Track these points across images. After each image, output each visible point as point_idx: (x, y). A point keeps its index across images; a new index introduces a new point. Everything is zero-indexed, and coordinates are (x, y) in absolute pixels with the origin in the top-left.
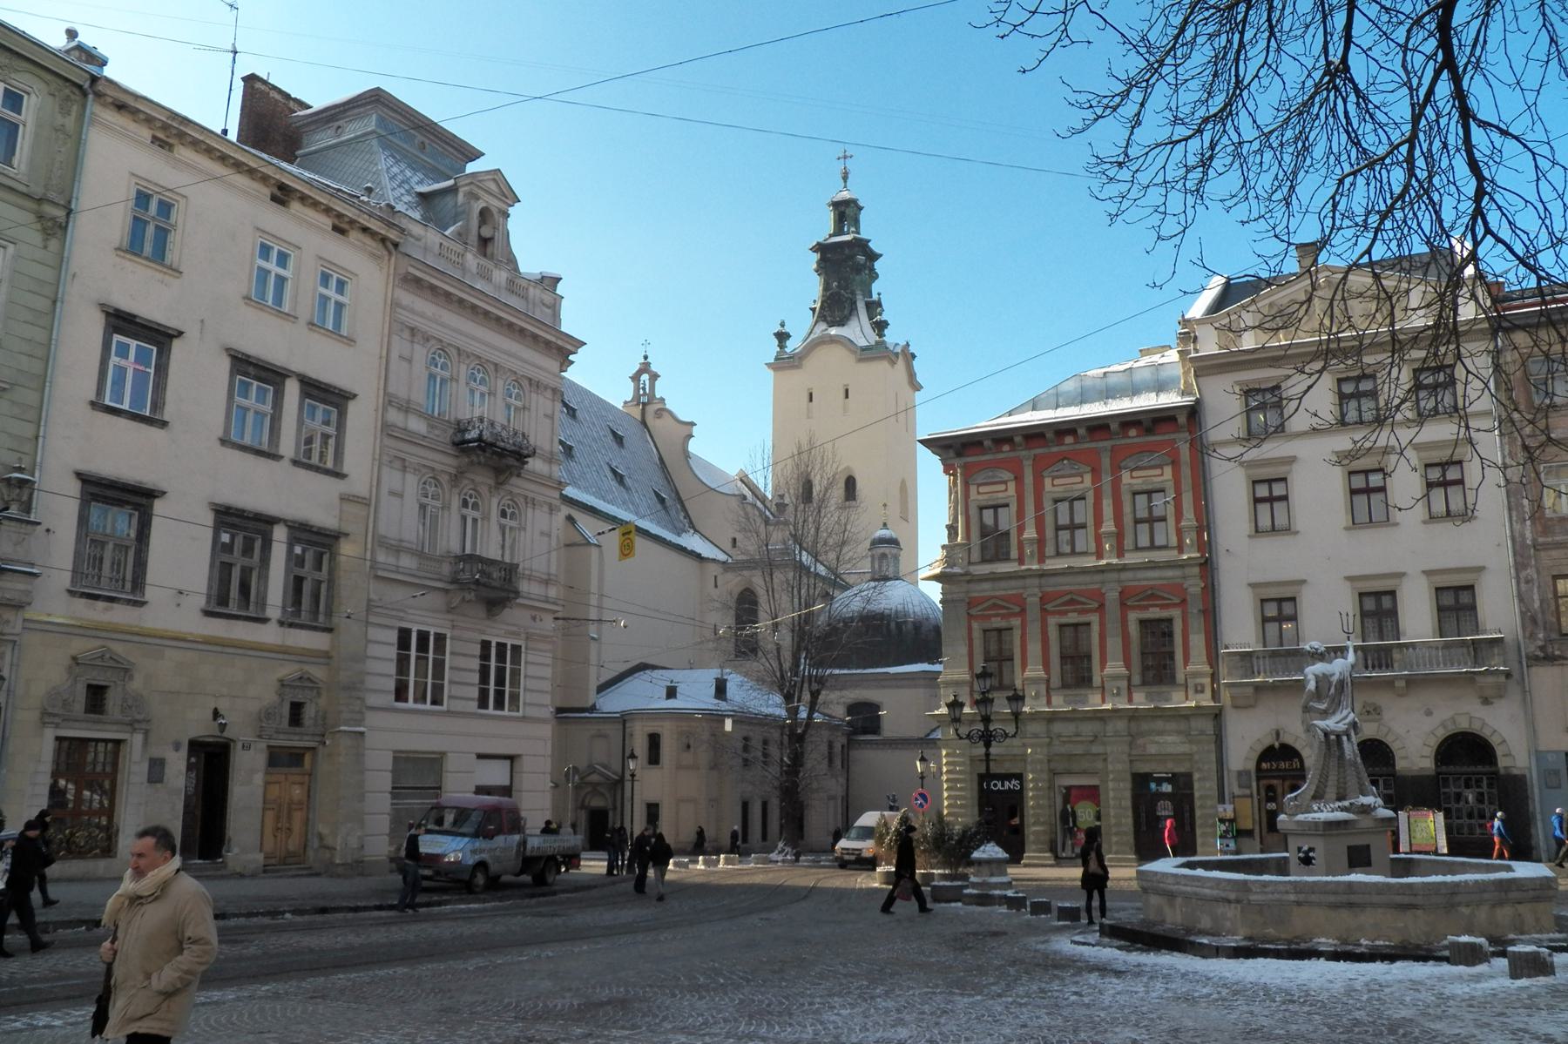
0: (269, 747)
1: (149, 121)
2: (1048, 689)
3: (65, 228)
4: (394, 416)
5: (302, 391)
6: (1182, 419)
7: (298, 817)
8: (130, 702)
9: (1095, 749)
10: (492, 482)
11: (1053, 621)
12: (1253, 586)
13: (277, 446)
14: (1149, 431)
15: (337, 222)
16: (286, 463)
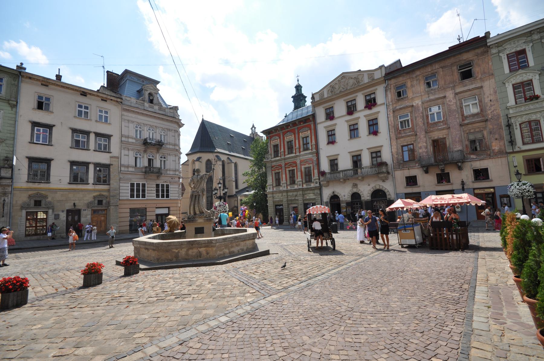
0: (92, 210)
1: (37, 80)
2: (287, 185)
3: (16, 106)
4: (123, 139)
5: (95, 136)
6: (311, 119)
7: (103, 224)
8: (47, 203)
9: (296, 198)
10: (157, 151)
11: (287, 169)
12: (327, 157)
13: (89, 147)
14: (305, 123)
15: (102, 98)
16: (91, 151)
